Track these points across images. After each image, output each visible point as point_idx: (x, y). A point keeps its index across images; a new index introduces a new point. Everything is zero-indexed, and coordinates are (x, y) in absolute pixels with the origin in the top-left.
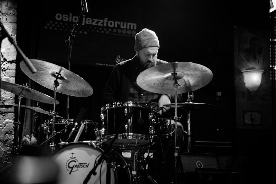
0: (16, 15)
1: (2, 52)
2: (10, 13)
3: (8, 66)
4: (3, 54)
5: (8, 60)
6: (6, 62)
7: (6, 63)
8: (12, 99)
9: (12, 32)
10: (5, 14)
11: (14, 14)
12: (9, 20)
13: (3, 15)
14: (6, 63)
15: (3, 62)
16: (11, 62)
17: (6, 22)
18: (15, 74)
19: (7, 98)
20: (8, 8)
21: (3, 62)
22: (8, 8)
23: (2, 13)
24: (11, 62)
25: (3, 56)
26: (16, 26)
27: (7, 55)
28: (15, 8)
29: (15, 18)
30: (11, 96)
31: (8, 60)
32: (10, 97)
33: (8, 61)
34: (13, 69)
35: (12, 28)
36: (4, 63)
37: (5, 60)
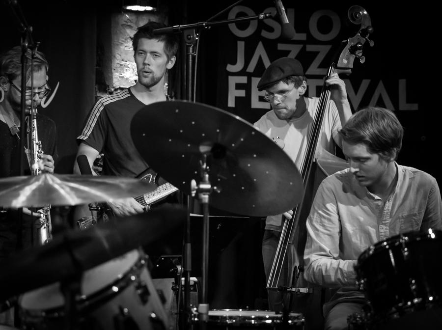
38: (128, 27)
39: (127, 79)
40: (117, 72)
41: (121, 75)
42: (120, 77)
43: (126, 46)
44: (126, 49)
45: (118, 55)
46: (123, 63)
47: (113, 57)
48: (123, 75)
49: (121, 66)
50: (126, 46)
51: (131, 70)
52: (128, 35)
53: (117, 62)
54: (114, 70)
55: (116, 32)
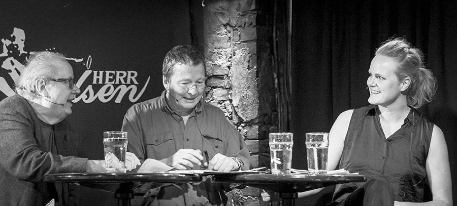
0: (254, 24)
1: (234, 106)
2: (245, 23)
3: (246, 132)
4: (236, 108)
5: (245, 120)
6: (243, 125)
7: (243, 127)
8: (254, 199)
9: (249, 61)
10: (236, 27)
11: (250, 22)
12: (244, 38)
13: (234, 30)
14: (243, 127)
15: (238, 125)
16: (249, 124)
17: (239, 43)
18: (257, 146)
19: (246, 198)
20: (241, 14)
21: (238, 126)
22: (241, 14)
23: (232, 27)
24: (249, 124)
25: (236, 113)
26: (255, 47)
27: (243, 110)
28: (253, 10)
29: (254, 30)
30: (253, 194)
31: (245, 120)
32: (251, 196)
33: (245, 122)
34: (254, 138)
35: (249, 53)
36: (239, 128)
37: (241, 121)
38: (220, 14)
39: (220, 66)
40: (210, 60)
41: (213, 63)
42: (213, 65)
43: (218, 34)
44: (219, 36)
45: (210, 44)
46: (215, 50)
47: (205, 46)
48: (216, 62)
49: (214, 54)
50: (218, 34)
51: (224, 57)
52: (220, 22)
53: (210, 50)
54: (207, 58)
55: (209, 21)
